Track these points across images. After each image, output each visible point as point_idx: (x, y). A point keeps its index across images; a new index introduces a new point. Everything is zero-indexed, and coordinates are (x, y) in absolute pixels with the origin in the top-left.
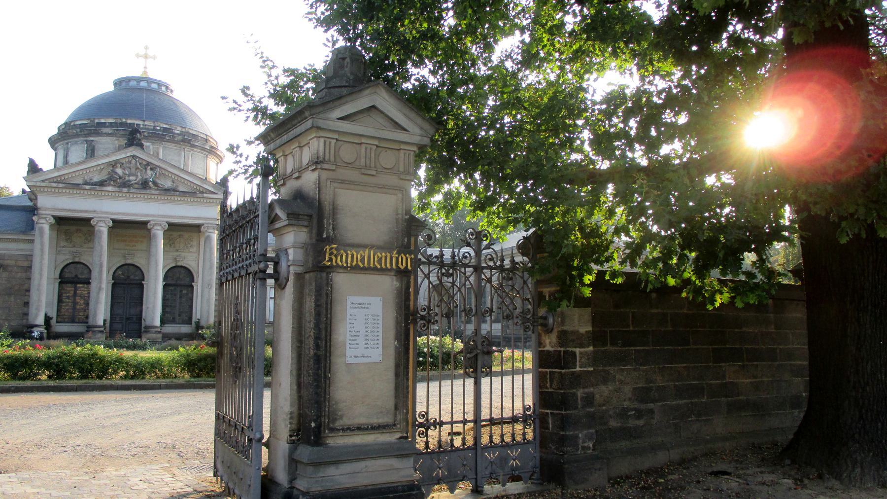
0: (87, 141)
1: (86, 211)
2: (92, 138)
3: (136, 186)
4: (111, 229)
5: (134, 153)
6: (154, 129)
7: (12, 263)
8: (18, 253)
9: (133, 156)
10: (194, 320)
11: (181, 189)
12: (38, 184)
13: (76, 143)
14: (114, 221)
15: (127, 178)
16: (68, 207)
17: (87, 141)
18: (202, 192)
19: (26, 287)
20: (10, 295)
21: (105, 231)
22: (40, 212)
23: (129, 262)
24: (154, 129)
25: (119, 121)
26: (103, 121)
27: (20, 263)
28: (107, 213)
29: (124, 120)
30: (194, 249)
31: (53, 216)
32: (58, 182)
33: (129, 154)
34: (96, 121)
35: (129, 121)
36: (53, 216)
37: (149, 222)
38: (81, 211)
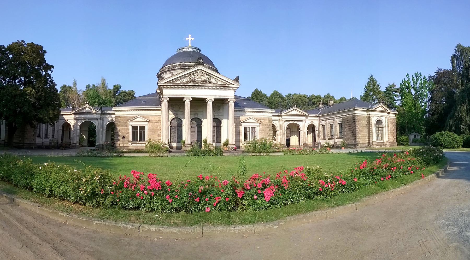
4: (191, 102)
5: (199, 68)
9: (198, 70)
11: (219, 83)
12: (163, 84)
19: (158, 128)
23: (196, 117)
27: (156, 119)
30: (221, 111)
33: (197, 69)
38: (180, 95)
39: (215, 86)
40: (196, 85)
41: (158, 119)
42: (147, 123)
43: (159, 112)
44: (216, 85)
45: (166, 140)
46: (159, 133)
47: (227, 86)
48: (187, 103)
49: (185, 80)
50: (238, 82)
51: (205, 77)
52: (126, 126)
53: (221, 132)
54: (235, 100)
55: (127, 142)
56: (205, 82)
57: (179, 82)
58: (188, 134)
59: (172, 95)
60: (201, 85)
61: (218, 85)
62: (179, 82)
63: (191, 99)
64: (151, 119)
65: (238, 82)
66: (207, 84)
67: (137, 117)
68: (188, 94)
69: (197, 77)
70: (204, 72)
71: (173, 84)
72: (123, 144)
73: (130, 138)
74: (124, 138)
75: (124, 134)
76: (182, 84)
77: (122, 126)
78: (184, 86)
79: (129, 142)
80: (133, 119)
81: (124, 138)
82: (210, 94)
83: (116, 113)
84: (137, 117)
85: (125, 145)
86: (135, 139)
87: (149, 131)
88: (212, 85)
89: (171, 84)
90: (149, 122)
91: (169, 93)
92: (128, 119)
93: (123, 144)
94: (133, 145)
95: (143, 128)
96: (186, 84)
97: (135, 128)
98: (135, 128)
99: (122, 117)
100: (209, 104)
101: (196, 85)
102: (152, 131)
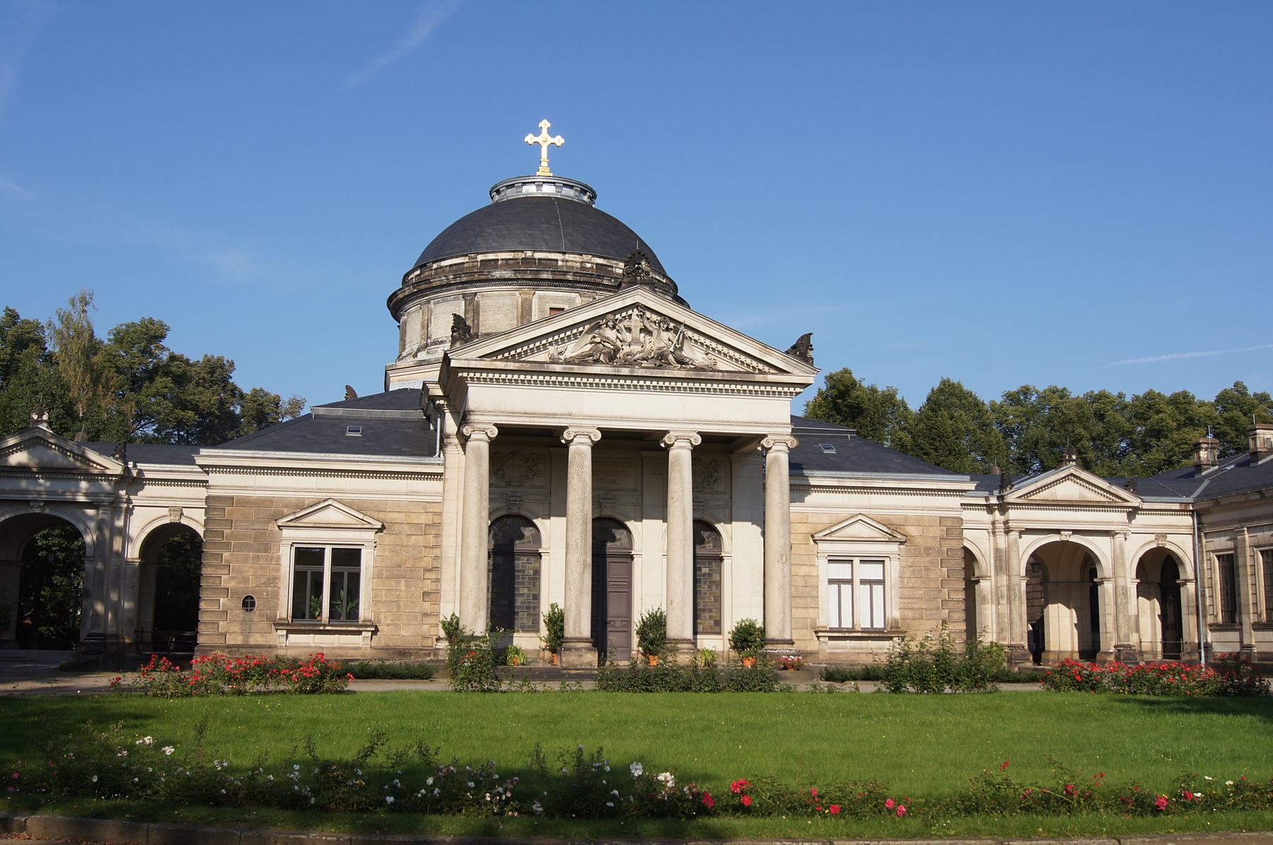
0: (464, 296)
1: (554, 415)
2: (473, 290)
3: (645, 363)
4: (596, 447)
6: (583, 268)
7: (399, 517)
8: (410, 498)
9: (635, 305)
10: (729, 625)
12: (473, 364)
13: (445, 299)
14: (604, 431)
15: (626, 349)
16: (508, 407)
17: (464, 296)
18: (761, 372)
19: (427, 562)
20: (397, 577)
21: (587, 450)
22: (473, 418)
24: (583, 268)
25: (521, 255)
26: (491, 256)
27: (415, 519)
28: (591, 417)
29: (529, 254)
30: (720, 487)
31: (495, 425)
32: (506, 359)
33: (629, 302)
34: (480, 257)
35: (538, 255)
36: (495, 425)
37: (666, 432)
38: (547, 415)
39: (703, 379)
40: (625, 371)
41: (423, 519)
42: (371, 535)
43: (435, 485)
44: (709, 375)
45: (475, 619)
46: (429, 586)
47: (759, 378)
48: (580, 454)
49: (572, 349)
50: (808, 360)
51: (664, 340)
52: (265, 545)
53: (719, 584)
54: (793, 443)
55: (265, 625)
56: (661, 359)
57: (542, 357)
58: (581, 593)
59: (513, 414)
60: (640, 372)
61: (719, 376)
62: (542, 357)
63: (598, 436)
64: (389, 517)
65: (808, 360)
66: (664, 369)
67: (318, 505)
68: (585, 412)
69: (628, 337)
70: (655, 317)
71: (518, 365)
72: (247, 633)
73: (285, 607)
74: (248, 603)
75: (251, 586)
76: (558, 368)
77: (241, 547)
78: (571, 374)
79: (278, 624)
80: (301, 511)
81: (248, 603)
82: (683, 416)
83: (213, 478)
84: (318, 505)
85: (257, 639)
86: (303, 614)
87: (378, 576)
88: (692, 375)
89: (512, 366)
90: (380, 530)
91: (497, 403)
92: (274, 512)
93: (247, 633)
94: (294, 638)
95: (348, 558)
96: (577, 369)
97: (307, 557)
98: (307, 557)
99: (245, 502)
100: (678, 458)
101: (625, 371)
102: (392, 573)
